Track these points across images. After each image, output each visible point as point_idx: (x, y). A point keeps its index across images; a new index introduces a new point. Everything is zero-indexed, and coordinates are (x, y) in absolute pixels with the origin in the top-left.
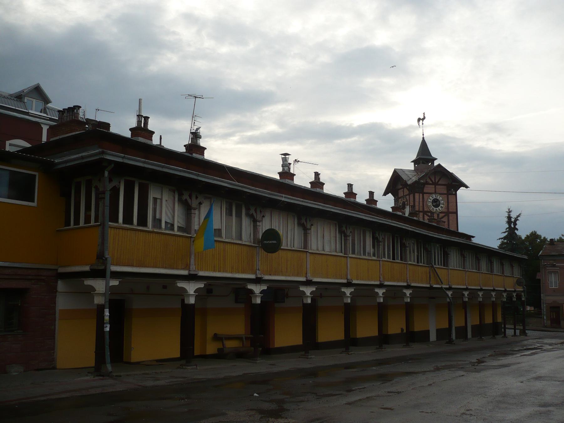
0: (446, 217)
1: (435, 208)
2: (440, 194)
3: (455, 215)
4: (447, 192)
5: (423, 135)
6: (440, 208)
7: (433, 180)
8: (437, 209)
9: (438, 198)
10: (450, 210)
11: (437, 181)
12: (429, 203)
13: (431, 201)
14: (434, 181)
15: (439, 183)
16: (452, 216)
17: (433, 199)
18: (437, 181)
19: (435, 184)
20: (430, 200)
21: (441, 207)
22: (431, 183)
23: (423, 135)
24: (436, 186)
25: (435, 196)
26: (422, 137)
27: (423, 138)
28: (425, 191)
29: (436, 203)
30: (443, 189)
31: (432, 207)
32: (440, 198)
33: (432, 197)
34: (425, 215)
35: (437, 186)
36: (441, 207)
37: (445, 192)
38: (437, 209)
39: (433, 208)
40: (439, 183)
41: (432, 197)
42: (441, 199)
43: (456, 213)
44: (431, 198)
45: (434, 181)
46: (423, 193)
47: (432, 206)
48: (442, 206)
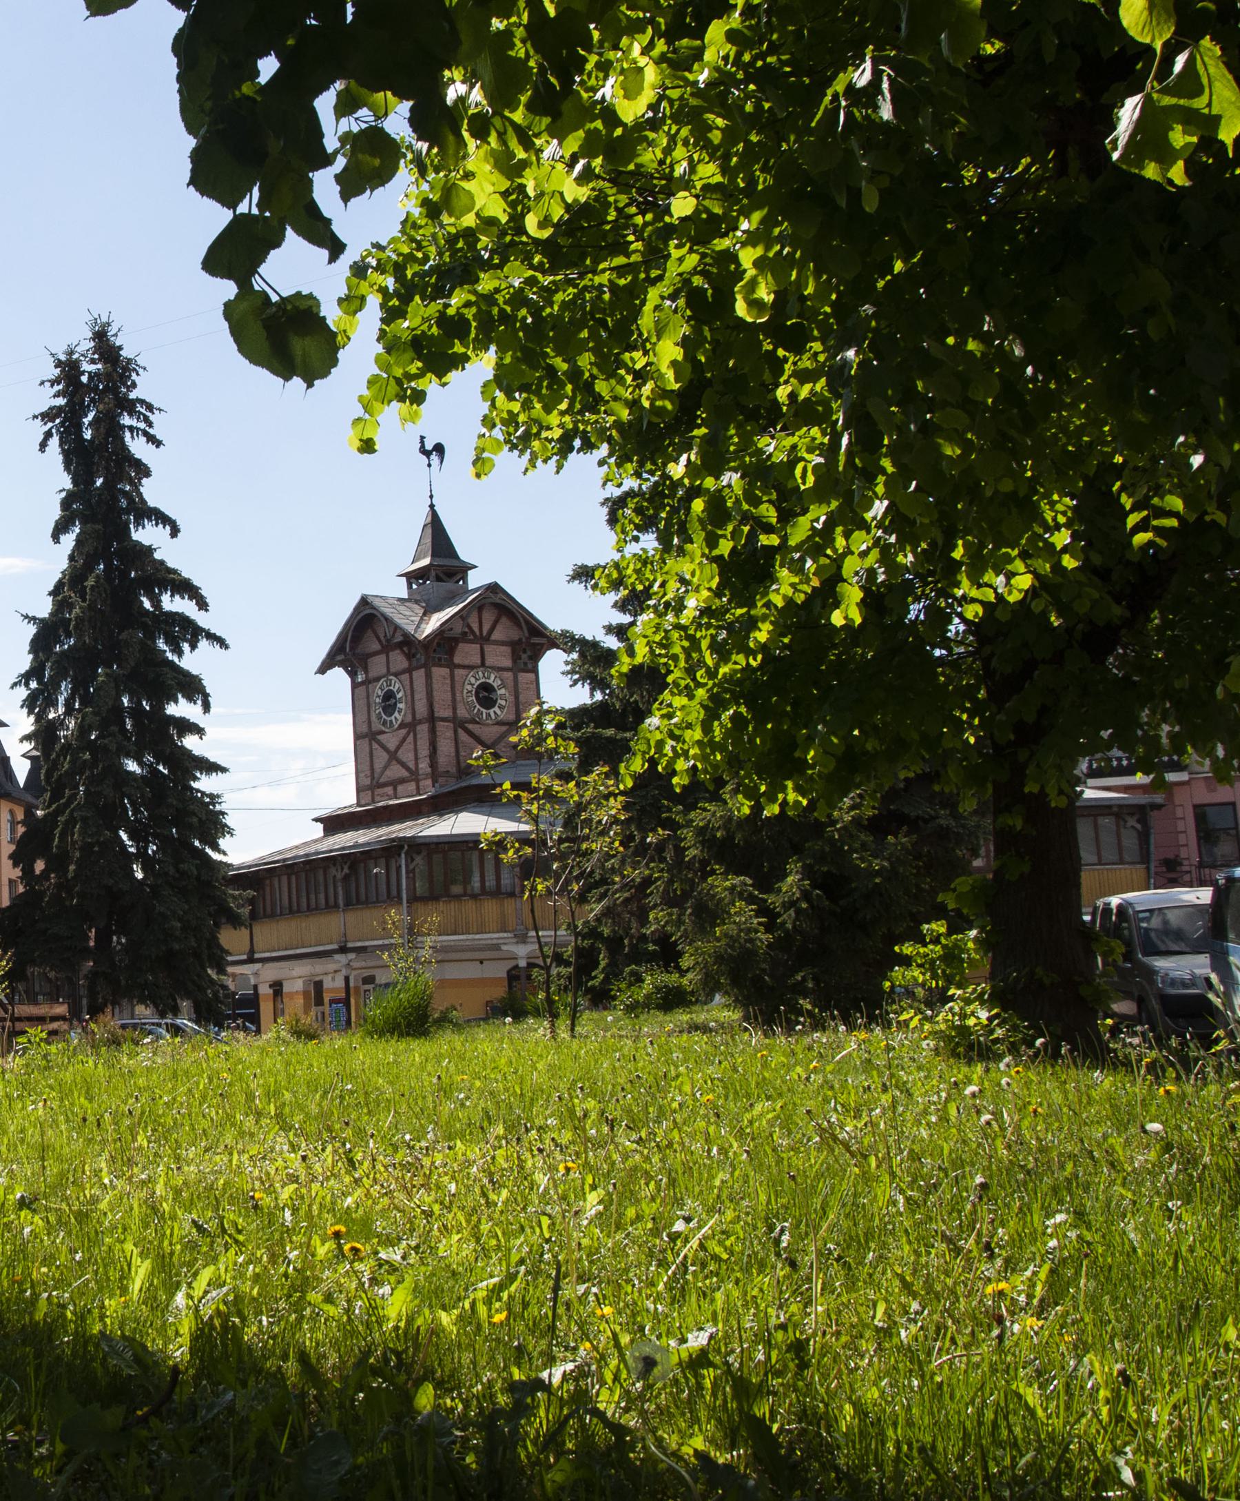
5: (431, 497)
6: (396, 714)
22: (376, 646)
23: (431, 497)
27: (432, 506)
32: (396, 686)
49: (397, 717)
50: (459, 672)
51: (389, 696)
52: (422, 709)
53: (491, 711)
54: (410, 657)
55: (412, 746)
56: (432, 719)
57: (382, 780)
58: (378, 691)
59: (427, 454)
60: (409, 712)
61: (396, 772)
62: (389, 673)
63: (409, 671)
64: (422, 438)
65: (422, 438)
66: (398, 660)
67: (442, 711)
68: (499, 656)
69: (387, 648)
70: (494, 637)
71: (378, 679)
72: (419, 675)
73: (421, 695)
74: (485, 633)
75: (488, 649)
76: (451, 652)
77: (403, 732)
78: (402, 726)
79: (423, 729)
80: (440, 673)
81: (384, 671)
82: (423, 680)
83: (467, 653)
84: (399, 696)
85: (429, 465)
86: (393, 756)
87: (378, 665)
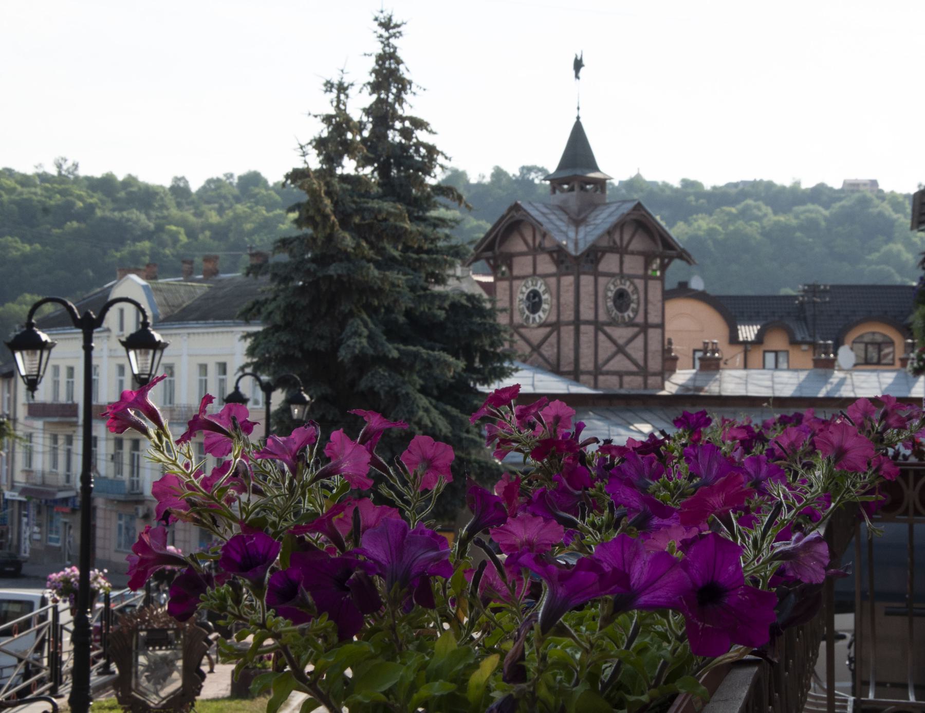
2: (545, 276)
5: (578, 108)
6: (541, 313)
8: (536, 316)
16: (567, 333)
17: (529, 290)
20: (521, 296)
21: (544, 311)
23: (578, 108)
25: (532, 285)
27: (578, 118)
28: (516, 272)
29: (534, 300)
31: (527, 312)
37: (552, 269)
42: (543, 288)
44: (524, 289)
49: (541, 316)
50: (602, 281)
51: (535, 294)
52: (568, 315)
53: (626, 315)
54: (558, 262)
56: (577, 322)
58: (523, 290)
63: (558, 275)
66: (546, 265)
67: (587, 313)
68: (633, 265)
69: (535, 250)
70: (632, 247)
71: (523, 278)
72: (568, 281)
73: (568, 297)
74: (625, 243)
75: (627, 259)
76: (596, 261)
77: (548, 329)
79: (567, 333)
80: (587, 281)
82: (572, 288)
83: (610, 263)
87: (522, 266)
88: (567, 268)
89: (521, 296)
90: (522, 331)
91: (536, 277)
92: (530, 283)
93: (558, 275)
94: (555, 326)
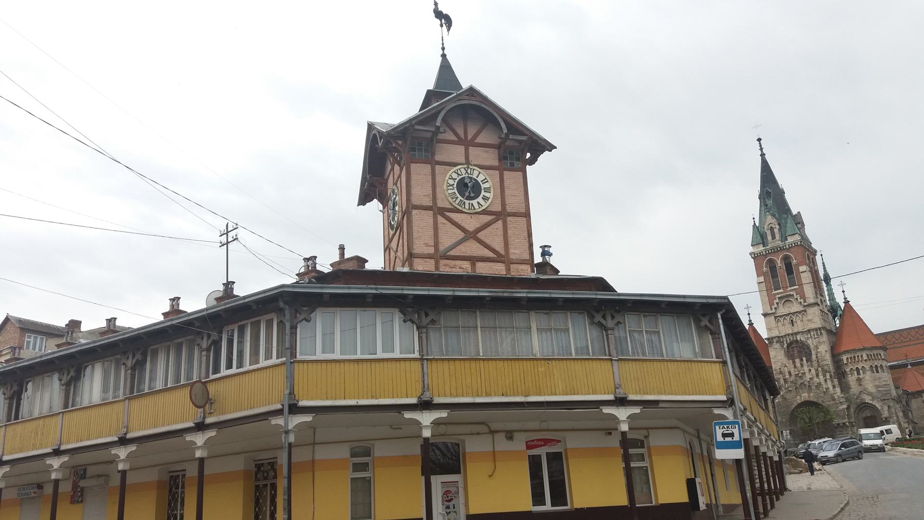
0: (500, 222)
1: (467, 202)
3: (524, 219)
4: (500, 160)
5: (443, 49)
6: (480, 199)
7: (461, 132)
8: (474, 202)
9: (474, 177)
10: (509, 209)
11: (469, 137)
12: (451, 187)
13: (456, 184)
14: (463, 137)
15: (475, 141)
17: (460, 177)
18: (469, 137)
19: (467, 143)
20: (451, 182)
21: (485, 199)
22: (454, 138)
23: (443, 49)
24: (470, 147)
25: (467, 172)
26: (441, 52)
27: (444, 56)
28: (438, 158)
29: (469, 188)
30: (490, 157)
31: (460, 198)
33: (458, 174)
34: (439, 216)
35: (471, 149)
36: (485, 199)
38: (472, 204)
39: (461, 200)
40: (475, 141)
41: (458, 174)
43: (527, 215)
44: (455, 176)
45: (463, 137)
46: (434, 163)
47: (458, 195)
48: (487, 195)
49: (479, 203)
55: (500, 232)
57: (452, 253)
59: (439, 14)
60: (499, 201)
61: (472, 248)
62: (468, 162)
64: (436, 4)
65: (436, 4)
71: (454, 165)
77: (489, 218)
78: (485, 212)
81: (464, 161)
84: (483, 186)
85: (442, 26)
86: (471, 235)
88: (512, 164)
89: (451, 182)
90: (453, 216)
91: (470, 167)
92: (463, 171)
93: (501, 169)
94: (501, 215)
